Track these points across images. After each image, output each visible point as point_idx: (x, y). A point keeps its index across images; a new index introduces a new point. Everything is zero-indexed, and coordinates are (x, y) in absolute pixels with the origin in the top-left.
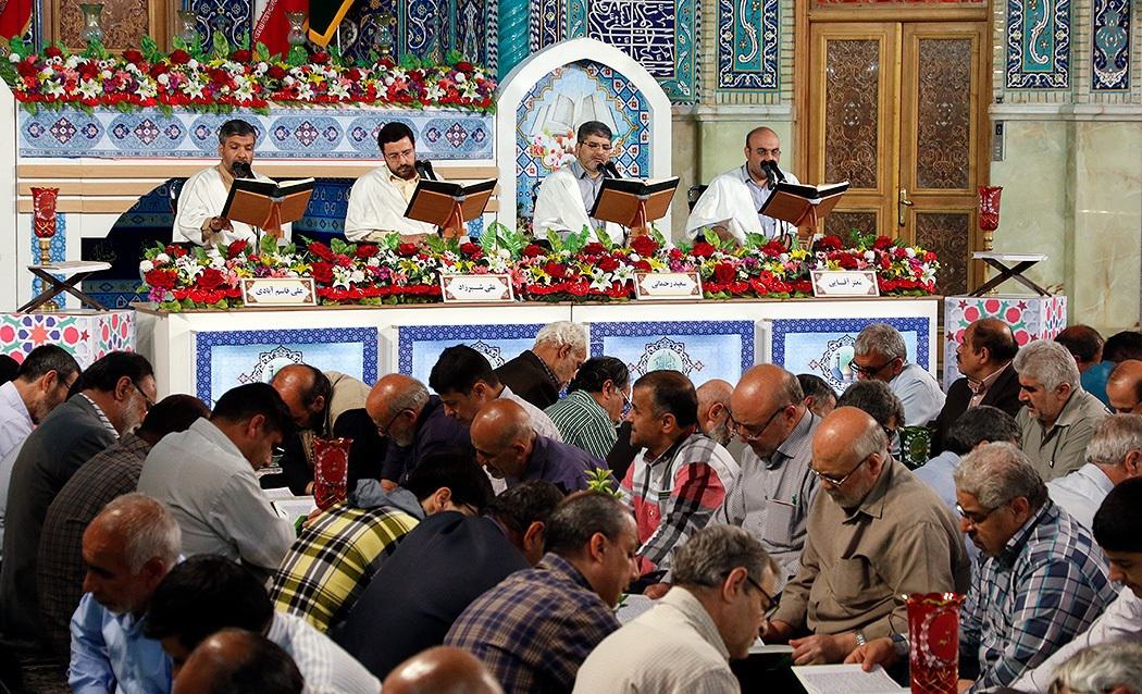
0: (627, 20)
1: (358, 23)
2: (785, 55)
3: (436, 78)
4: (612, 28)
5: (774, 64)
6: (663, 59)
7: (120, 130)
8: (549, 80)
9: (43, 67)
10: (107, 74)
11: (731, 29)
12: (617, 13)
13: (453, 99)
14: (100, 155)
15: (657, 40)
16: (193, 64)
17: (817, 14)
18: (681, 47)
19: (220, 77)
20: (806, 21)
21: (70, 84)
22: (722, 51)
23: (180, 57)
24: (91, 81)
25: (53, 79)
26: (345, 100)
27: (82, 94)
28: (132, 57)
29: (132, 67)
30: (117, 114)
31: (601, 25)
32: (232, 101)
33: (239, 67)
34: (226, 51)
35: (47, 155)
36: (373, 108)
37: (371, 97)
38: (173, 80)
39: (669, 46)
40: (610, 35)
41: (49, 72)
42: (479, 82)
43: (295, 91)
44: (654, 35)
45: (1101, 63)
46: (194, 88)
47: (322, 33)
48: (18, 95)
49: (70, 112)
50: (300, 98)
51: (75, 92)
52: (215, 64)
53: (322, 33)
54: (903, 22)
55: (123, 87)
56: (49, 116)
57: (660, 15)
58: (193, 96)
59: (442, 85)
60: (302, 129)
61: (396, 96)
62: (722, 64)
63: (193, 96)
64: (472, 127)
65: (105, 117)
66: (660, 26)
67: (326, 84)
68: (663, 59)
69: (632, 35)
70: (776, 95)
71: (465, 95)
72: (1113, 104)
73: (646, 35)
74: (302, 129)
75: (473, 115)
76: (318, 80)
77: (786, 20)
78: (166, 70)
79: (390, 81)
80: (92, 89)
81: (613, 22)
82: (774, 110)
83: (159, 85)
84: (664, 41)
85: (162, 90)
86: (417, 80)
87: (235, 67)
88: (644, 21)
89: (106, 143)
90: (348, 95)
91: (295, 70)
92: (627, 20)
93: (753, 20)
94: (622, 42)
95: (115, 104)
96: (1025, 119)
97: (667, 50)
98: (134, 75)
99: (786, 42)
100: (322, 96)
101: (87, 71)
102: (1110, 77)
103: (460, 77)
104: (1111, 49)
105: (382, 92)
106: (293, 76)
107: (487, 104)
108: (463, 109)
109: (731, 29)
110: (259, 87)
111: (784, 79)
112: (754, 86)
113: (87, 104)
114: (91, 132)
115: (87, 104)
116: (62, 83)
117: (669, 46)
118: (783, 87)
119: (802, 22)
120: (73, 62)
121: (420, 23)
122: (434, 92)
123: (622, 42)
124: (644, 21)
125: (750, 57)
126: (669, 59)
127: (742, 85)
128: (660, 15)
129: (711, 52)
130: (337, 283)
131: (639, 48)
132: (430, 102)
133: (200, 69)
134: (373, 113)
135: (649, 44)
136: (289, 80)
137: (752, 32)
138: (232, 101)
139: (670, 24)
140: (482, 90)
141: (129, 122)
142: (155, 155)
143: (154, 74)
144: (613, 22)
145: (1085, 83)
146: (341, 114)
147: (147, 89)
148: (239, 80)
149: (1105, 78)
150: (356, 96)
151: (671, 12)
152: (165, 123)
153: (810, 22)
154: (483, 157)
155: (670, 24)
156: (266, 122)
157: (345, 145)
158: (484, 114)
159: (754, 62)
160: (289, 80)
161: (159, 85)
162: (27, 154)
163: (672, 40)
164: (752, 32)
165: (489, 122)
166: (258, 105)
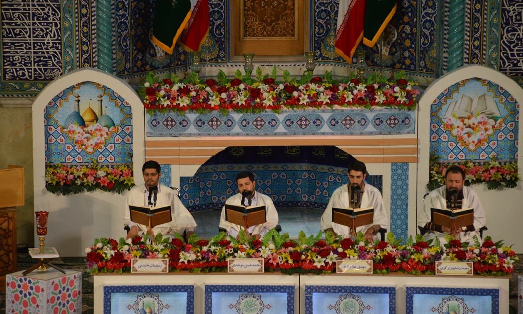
1: (398, 29)
4: (516, 48)
7: (200, 123)
10: (193, 94)
16: (242, 87)
21: (174, 99)
25: (164, 97)
26: (327, 104)
27: (179, 104)
29: (208, 89)
30: (198, 115)
31: (509, 47)
33: (266, 87)
36: (344, 108)
37: (342, 102)
38: (229, 96)
40: (515, 52)
41: (162, 93)
43: (298, 100)
48: (146, 106)
50: (301, 103)
51: (175, 104)
52: (255, 85)
55: (201, 101)
58: (240, 104)
59: (385, 94)
63: (240, 104)
64: (402, 117)
67: (318, 94)
71: (399, 100)
74: (301, 120)
75: (403, 111)
79: (355, 92)
80: (184, 102)
83: (221, 99)
85: (222, 101)
90: (329, 101)
95: (197, 109)
98: (208, 94)
100: (314, 102)
101: (184, 92)
103: (397, 89)
105: (350, 98)
120: (176, 88)
121: (427, 32)
130: (181, 261)
133: (245, 89)
134: (342, 111)
140: (409, 95)
141: (204, 118)
142: (219, 135)
146: (323, 111)
147: (214, 101)
150: (334, 100)
152: (225, 119)
154: (409, 133)
157: (326, 128)
158: (410, 110)
165: (413, 114)
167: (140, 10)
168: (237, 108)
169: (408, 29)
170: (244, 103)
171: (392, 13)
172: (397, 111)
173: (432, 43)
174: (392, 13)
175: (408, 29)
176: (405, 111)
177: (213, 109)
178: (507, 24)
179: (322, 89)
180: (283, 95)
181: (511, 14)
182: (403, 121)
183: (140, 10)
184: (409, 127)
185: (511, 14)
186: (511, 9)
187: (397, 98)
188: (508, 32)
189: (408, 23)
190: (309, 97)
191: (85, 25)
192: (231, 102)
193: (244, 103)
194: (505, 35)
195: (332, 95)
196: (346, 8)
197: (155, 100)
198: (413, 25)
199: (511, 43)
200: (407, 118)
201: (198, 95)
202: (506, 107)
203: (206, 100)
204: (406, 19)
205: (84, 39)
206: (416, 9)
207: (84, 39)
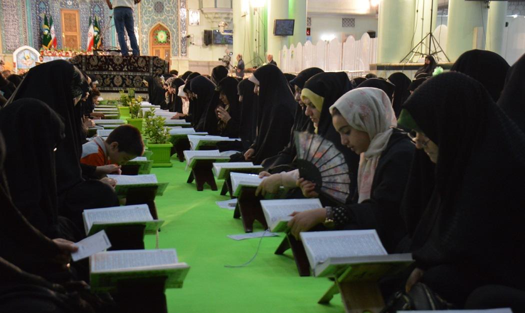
19: (67, 53)
23: (62, 51)
28: (56, 51)
45: (182, 53)
49: (47, 57)
54: (163, 47)
72: (184, 58)
77: (149, 47)
80: (50, 54)
87: (69, 52)
96: (175, 60)
102: (184, 54)
104: (184, 50)
113: (49, 56)
119: (151, 48)
145: (180, 55)
149: (183, 54)
153: (153, 48)
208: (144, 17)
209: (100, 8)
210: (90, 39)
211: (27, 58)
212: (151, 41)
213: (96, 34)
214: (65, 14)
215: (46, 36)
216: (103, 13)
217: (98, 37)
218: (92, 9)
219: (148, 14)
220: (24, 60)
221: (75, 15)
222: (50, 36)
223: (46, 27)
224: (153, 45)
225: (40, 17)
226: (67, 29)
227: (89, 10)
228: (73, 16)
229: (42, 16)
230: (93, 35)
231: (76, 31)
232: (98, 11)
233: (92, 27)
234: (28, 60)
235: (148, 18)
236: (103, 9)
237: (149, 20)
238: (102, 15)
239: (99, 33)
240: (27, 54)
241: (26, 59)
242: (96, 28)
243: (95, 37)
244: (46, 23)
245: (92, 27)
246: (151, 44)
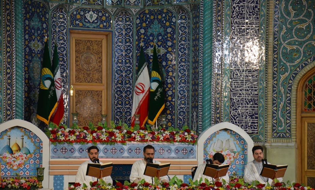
0: (242, 117)
2: (293, 127)
3: (179, 134)
4: (237, 119)
5: (290, 130)
6: (254, 128)
8: (215, 134)
9: (58, 132)
10: (78, 133)
11: (276, 119)
12: (239, 114)
13: (184, 140)
14: (75, 157)
15: (252, 123)
16: (104, 130)
17: (304, 115)
18: (260, 125)
20: (300, 117)
21: (67, 136)
22: (273, 126)
23: (100, 128)
24: (73, 135)
25: (61, 135)
26: (150, 141)
27: (70, 139)
29: (85, 131)
30: (80, 145)
31: (234, 118)
32: (115, 141)
33: (118, 131)
34: (114, 126)
35: (59, 158)
38: (97, 135)
39: (256, 124)
40: (237, 121)
41: (60, 133)
42: (192, 135)
43: (135, 138)
44: (251, 121)
46: (104, 137)
47: (152, 121)
48: (51, 140)
49: (66, 145)
50: (136, 140)
52: (110, 130)
53: (152, 121)
55: (82, 137)
56: (60, 146)
57: (253, 115)
58: (103, 140)
59: (180, 136)
60: (136, 149)
61: (166, 140)
62: (273, 130)
63: (103, 140)
64: (189, 149)
65: (77, 146)
66: (253, 118)
67: (144, 136)
68: (254, 128)
69: (244, 121)
70: (290, 140)
71: (187, 139)
73: (249, 121)
74: (136, 149)
75: (190, 145)
76: (142, 135)
77: (293, 116)
78: (95, 132)
79: (164, 135)
80: (73, 138)
81: (238, 117)
82: (290, 144)
83: (93, 136)
84: (255, 123)
85: (94, 138)
86: (172, 134)
88: (248, 117)
89: (77, 154)
90: (151, 139)
91: (135, 132)
92: (242, 117)
93: (283, 116)
94: (241, 123)
95: (80, 142)
97: (256, 126)
98: (86, 134)
99: (293, 123)
101: (72, 133)
103: (186, 134)
105: (162, 138)
106: (134, 134)
107: (194, 141)
108: (187, 143)
109: (276, 119)
110: (124, 137)
111: (293, 135)
112: (283, 137)
113: (71, 142)
114: (72, 151)
115: (71, 142)
116: (64, 136)
117: (256, 124)
118: (293, 137)
119: (299, 117)
120: (67, 130)
122: (178, 138)
123: (241, 123)
124: (248, 117)
125: (282, 128)
126: (256, 128)
127: (279, 137)
128: (253, 115)
129: (270, 126)
131: (246, 125)
132: (177, 141)
133: (106, 132)
134: (159, 145)
135: (250, 124)
136: (133, 135)
137: (283, 120)
138: (115, 141)
139: (257, 118)
140: (193, 137)
143: (92, 133)
144: (238, 117)
147: (89, 138)
148: (117, 135)
151: (257, 114)
153: (302, 117)
154: (193, 158)
155: (257, 118)
156: (126, 147)
158: (193, 145)
159: (284, 129)
160: (133, 135)
161: (93, 136)
162: (53, 157)
163: (257, 123)
164: (283, 120)
165: (195, 147)
166: (123, 142)
167: (27, 103)
168: (101, 141)
169: (169, 117)
170: (106, 139)
171: (163, 107)
172: (187, 146)
173: (184, 123)
174: (163, 107)
175: (169, 117)
176: (191, 146)
177: (88, 142)
178: (233, 106)
179: (147, 133)
180: (126, 136)
181: (234, 101)
182: (190, 151)
183: (27, 103)
184: (193, 155)
185: (234, 101)
186: (235, 98)
187: (186, 138)
188: (233, 110)
189: (170, 114)
190: (140, 136)
191: (9, 99)
192: (99, 138)
193: (106, 139)
194: (232, 112)
195: (153, 136)
196: (137, 105)
197: (56, 137)
198: (172, 114)
199: (235, 116)
200: (192, 150)
201: (80, 135)
202: (239, 146)
203: (85, 137)
204: (168, 112)
205: (8, 108)
206: (174, 106)
207: (8, 108)
208: (284, 44)
209: (166, 28)
210: (137, 100)
211: (14, 149)
212: (299, 102)
213: (155, 85)
214: (78, 43)
215: (44, 93)
216: (172, 39)
217: (158, 94)
218: (142, 31)
219: (296, 38)
220: (8, 155)
221: (100, 43)
222: (54, 92)
223: (47, 71)
224: (302, 112)
225: (30, 49)
226: (81, 76)
227: (135, 30)
228: (96, 47)
229: (37, 46)
230: (146, 89)
231: (100, 80)
232: (160, 34)
233: (145, 71)
234: (17, 154)
235: (295, 47)
236: (174, 31)
237: (298, 51)
238: (170, 44)
239: (162, 84)
240: (16, 138)
241: (11, 152)
242: (155, 74)
243: (151, 94)
244: (45, 64)
245: (145, 71)
246: (299, 109)
